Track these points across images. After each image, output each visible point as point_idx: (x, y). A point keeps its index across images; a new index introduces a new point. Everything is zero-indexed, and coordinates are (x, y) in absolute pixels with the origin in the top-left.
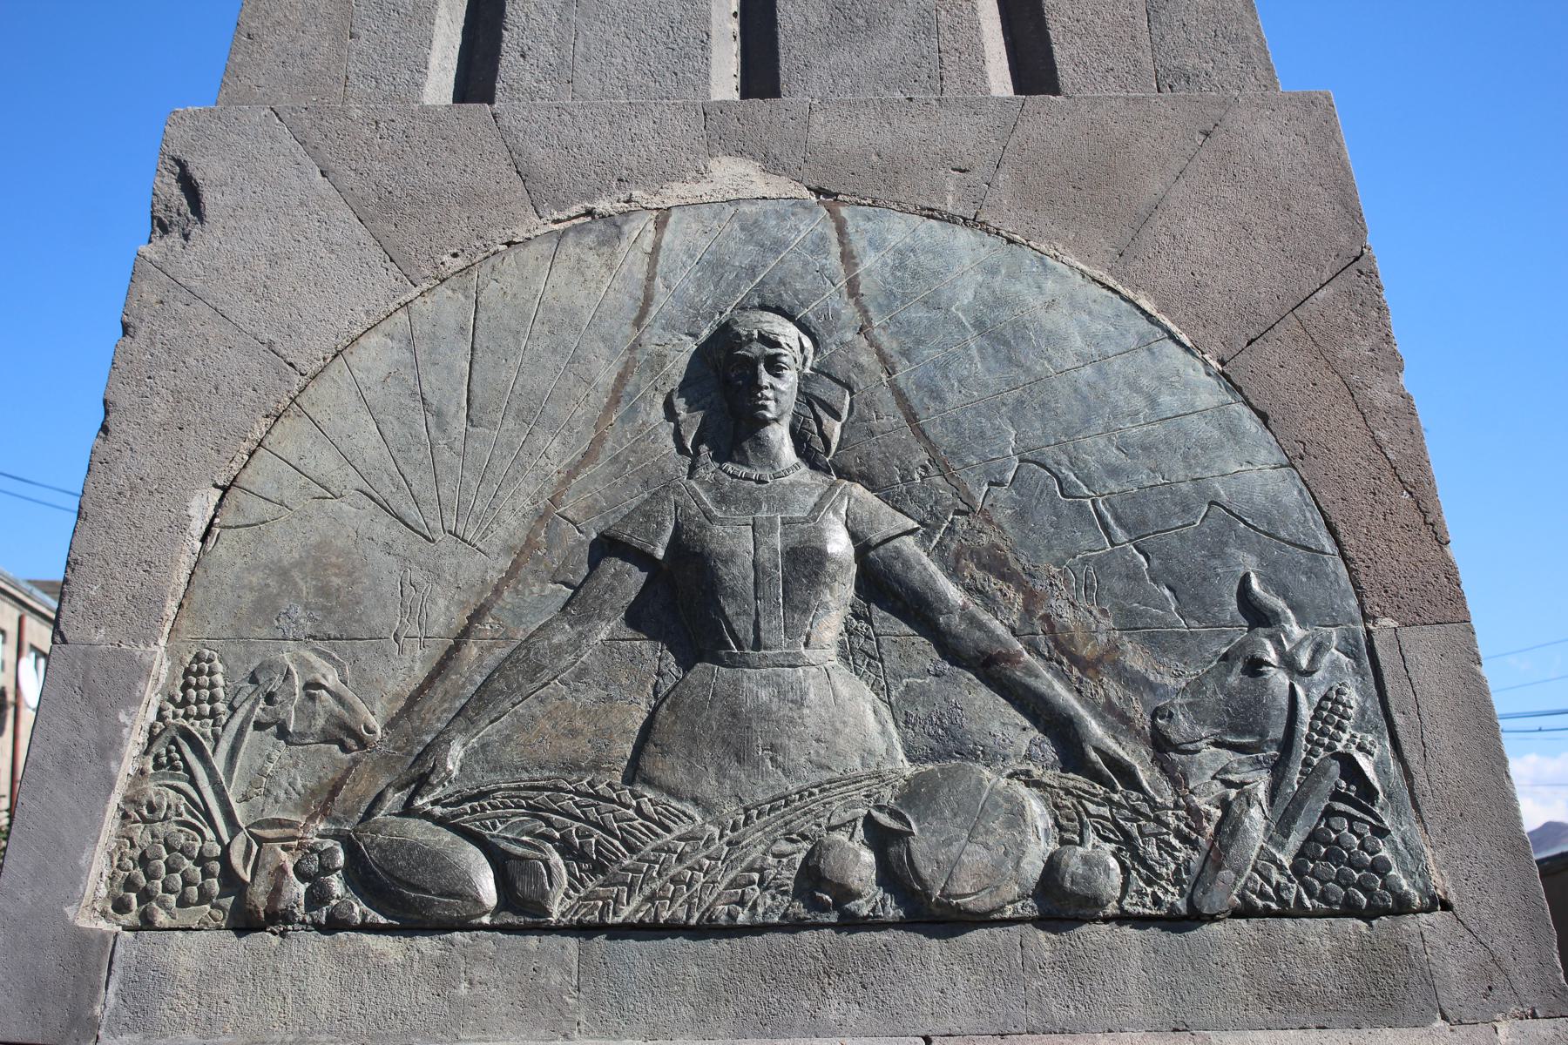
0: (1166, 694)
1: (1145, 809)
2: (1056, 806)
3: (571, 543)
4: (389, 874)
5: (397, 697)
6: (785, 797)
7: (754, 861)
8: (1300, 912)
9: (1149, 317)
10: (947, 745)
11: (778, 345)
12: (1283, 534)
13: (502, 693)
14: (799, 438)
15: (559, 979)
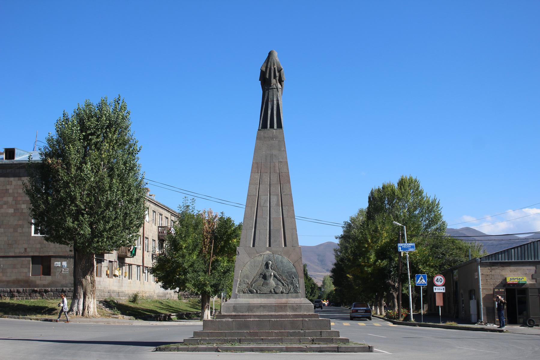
10: (277, 284)
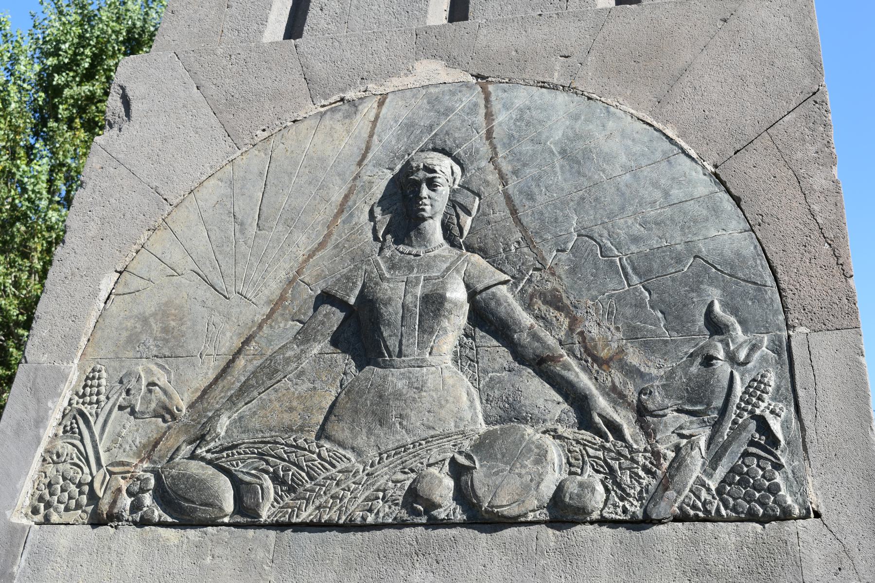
0: (652, 379)
1: (626, 452)
2: (569, 451)
3: (305, 296)
4: (175, 493)
5: (197, 390)
6: (404, 446)
7: (380, 486)
8: (719, 518)
9: (671, 140)
10: (510, 414)
11: (435, 171)
12: (740, 275)
13: (253, 386)
14: (446, 228)
15: (262, 555)
